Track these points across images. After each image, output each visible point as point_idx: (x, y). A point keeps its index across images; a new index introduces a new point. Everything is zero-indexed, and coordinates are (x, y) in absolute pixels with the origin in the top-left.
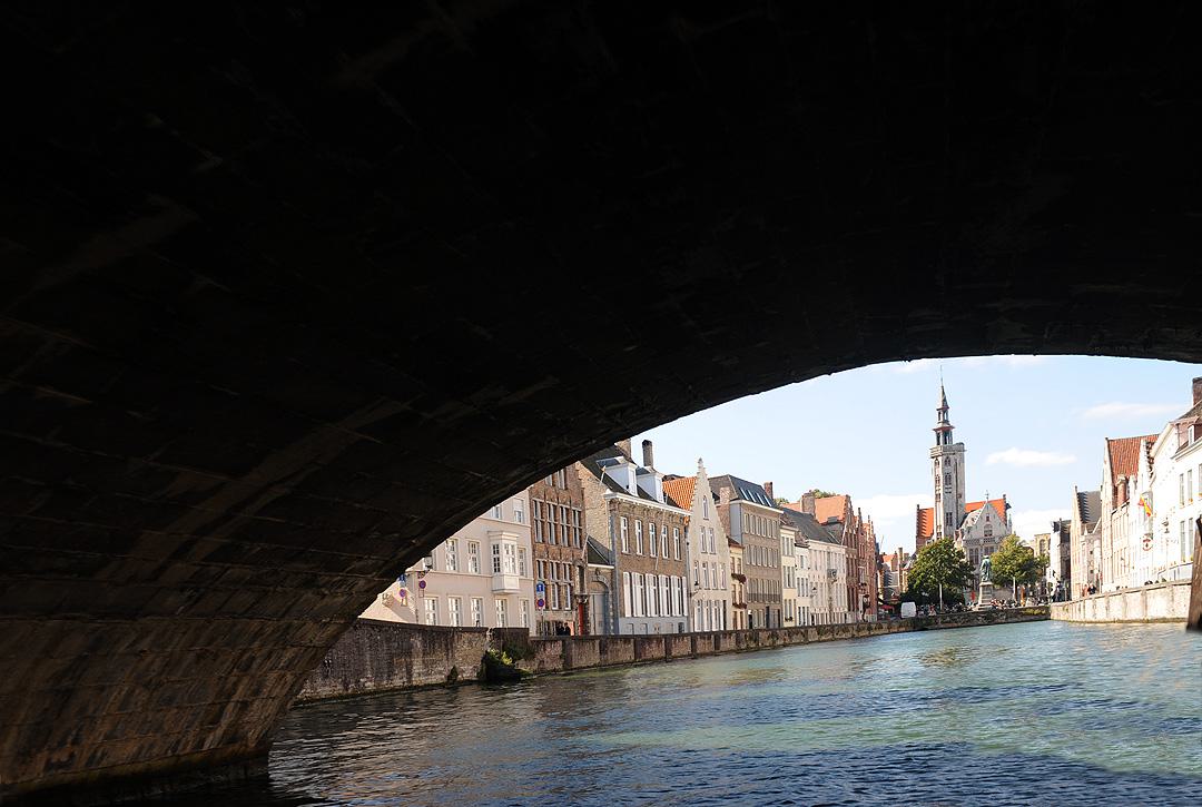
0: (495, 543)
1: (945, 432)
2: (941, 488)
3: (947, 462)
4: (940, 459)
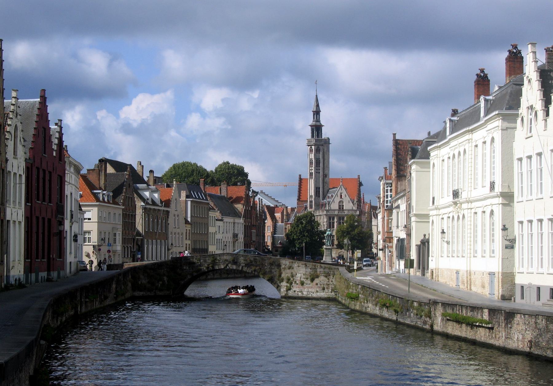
1: (317, 129)
2: (313, 168)
4: (313, 147)
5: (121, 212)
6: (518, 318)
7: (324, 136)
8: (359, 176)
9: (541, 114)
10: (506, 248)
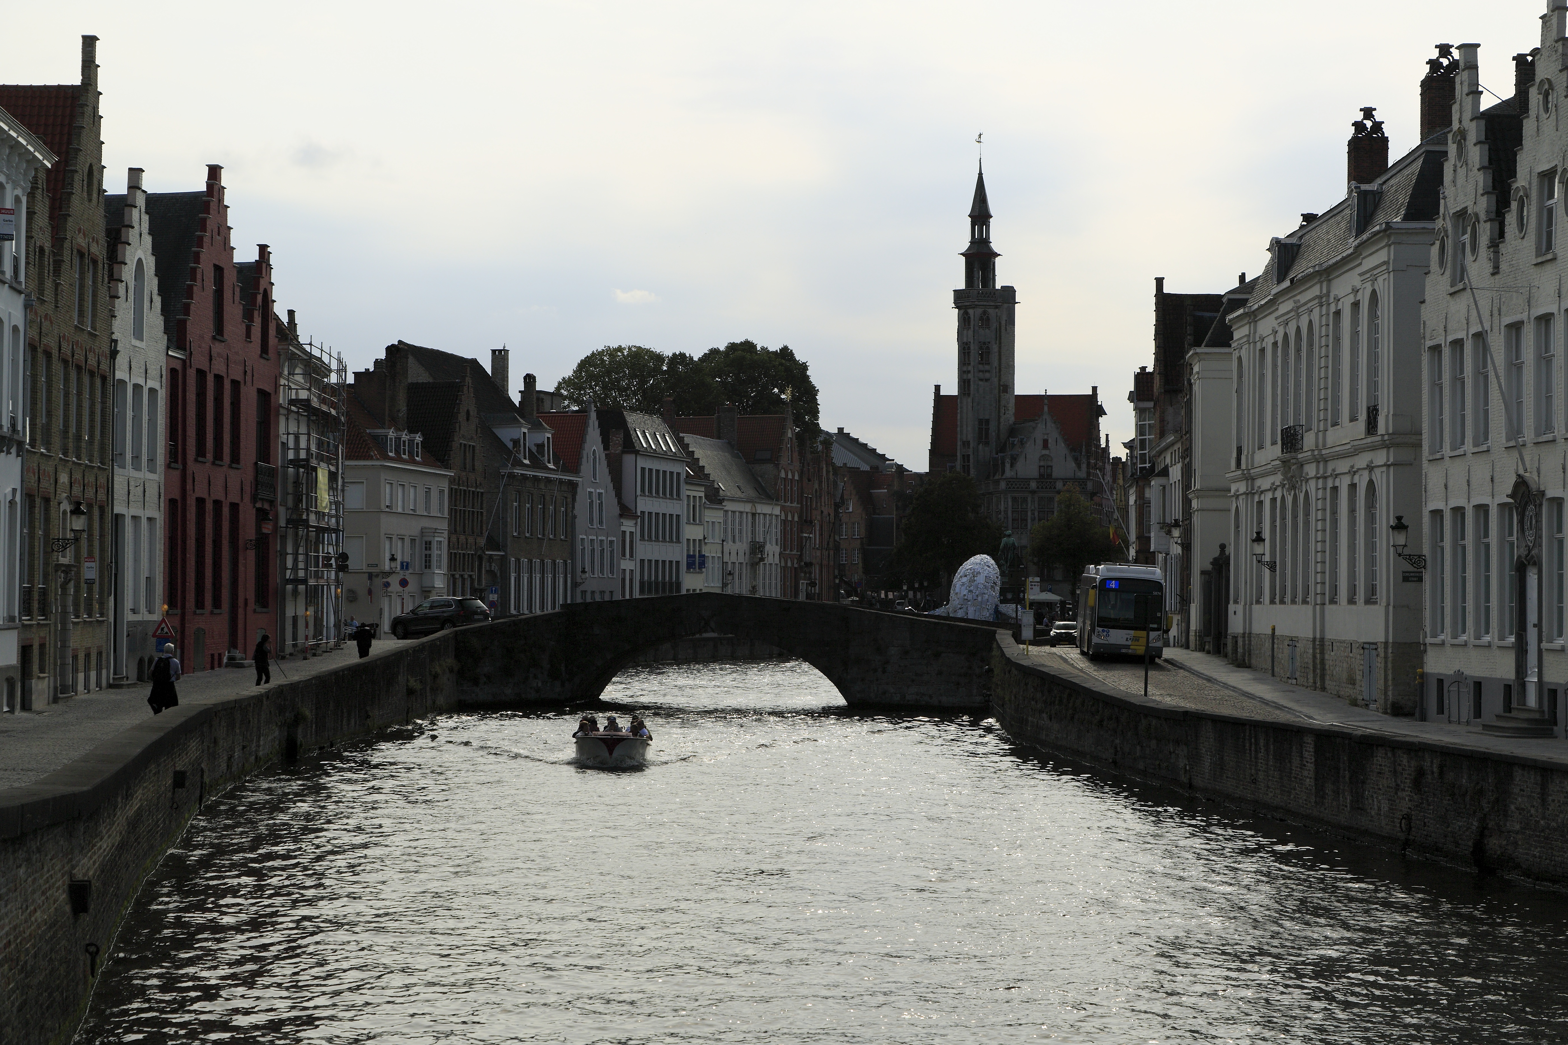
0: (428, 539)
3: (985, 320)
5: (445, 485)
6: (1380, 759)
7: (1000, 282)
8: (1095, 389)
9: (1485, 232)
10: (1406, 579)
